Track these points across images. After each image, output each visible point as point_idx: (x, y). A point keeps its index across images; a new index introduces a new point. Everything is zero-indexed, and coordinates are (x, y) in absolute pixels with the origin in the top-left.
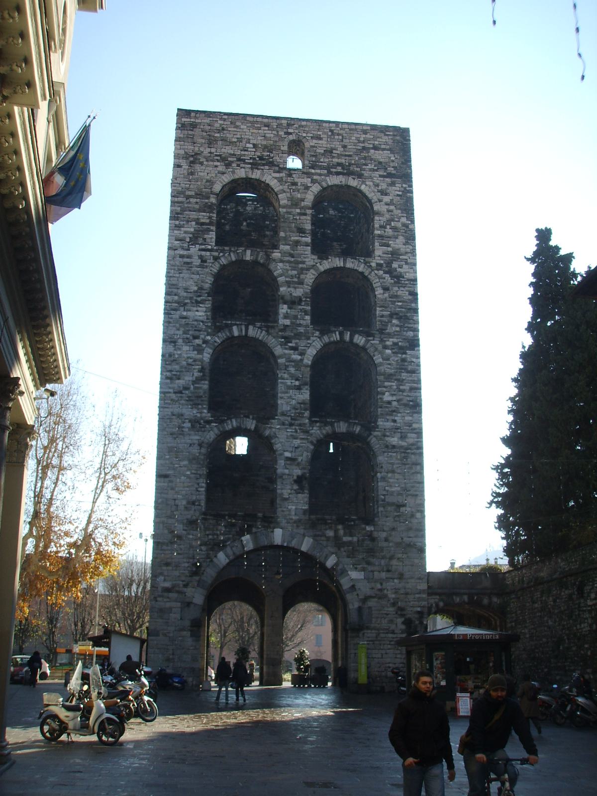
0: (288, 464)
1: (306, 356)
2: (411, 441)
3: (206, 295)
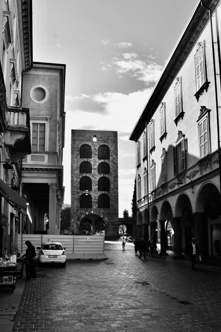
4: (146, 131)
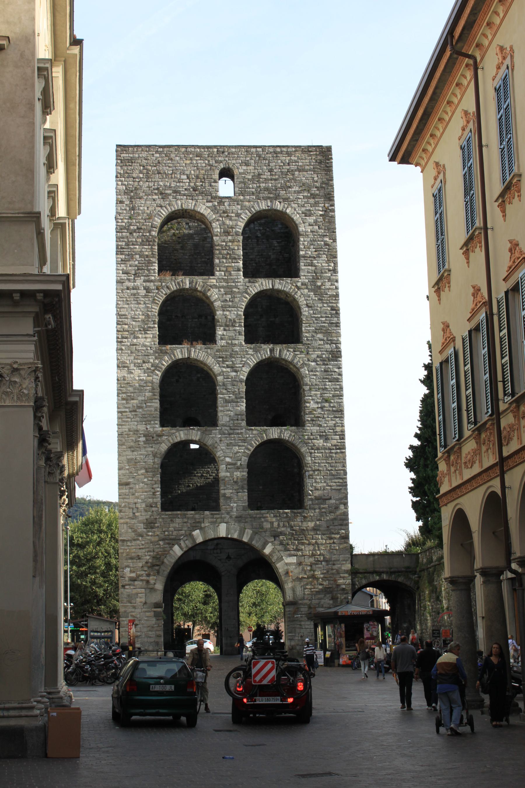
2: (334, 442)
4: (472, 109)
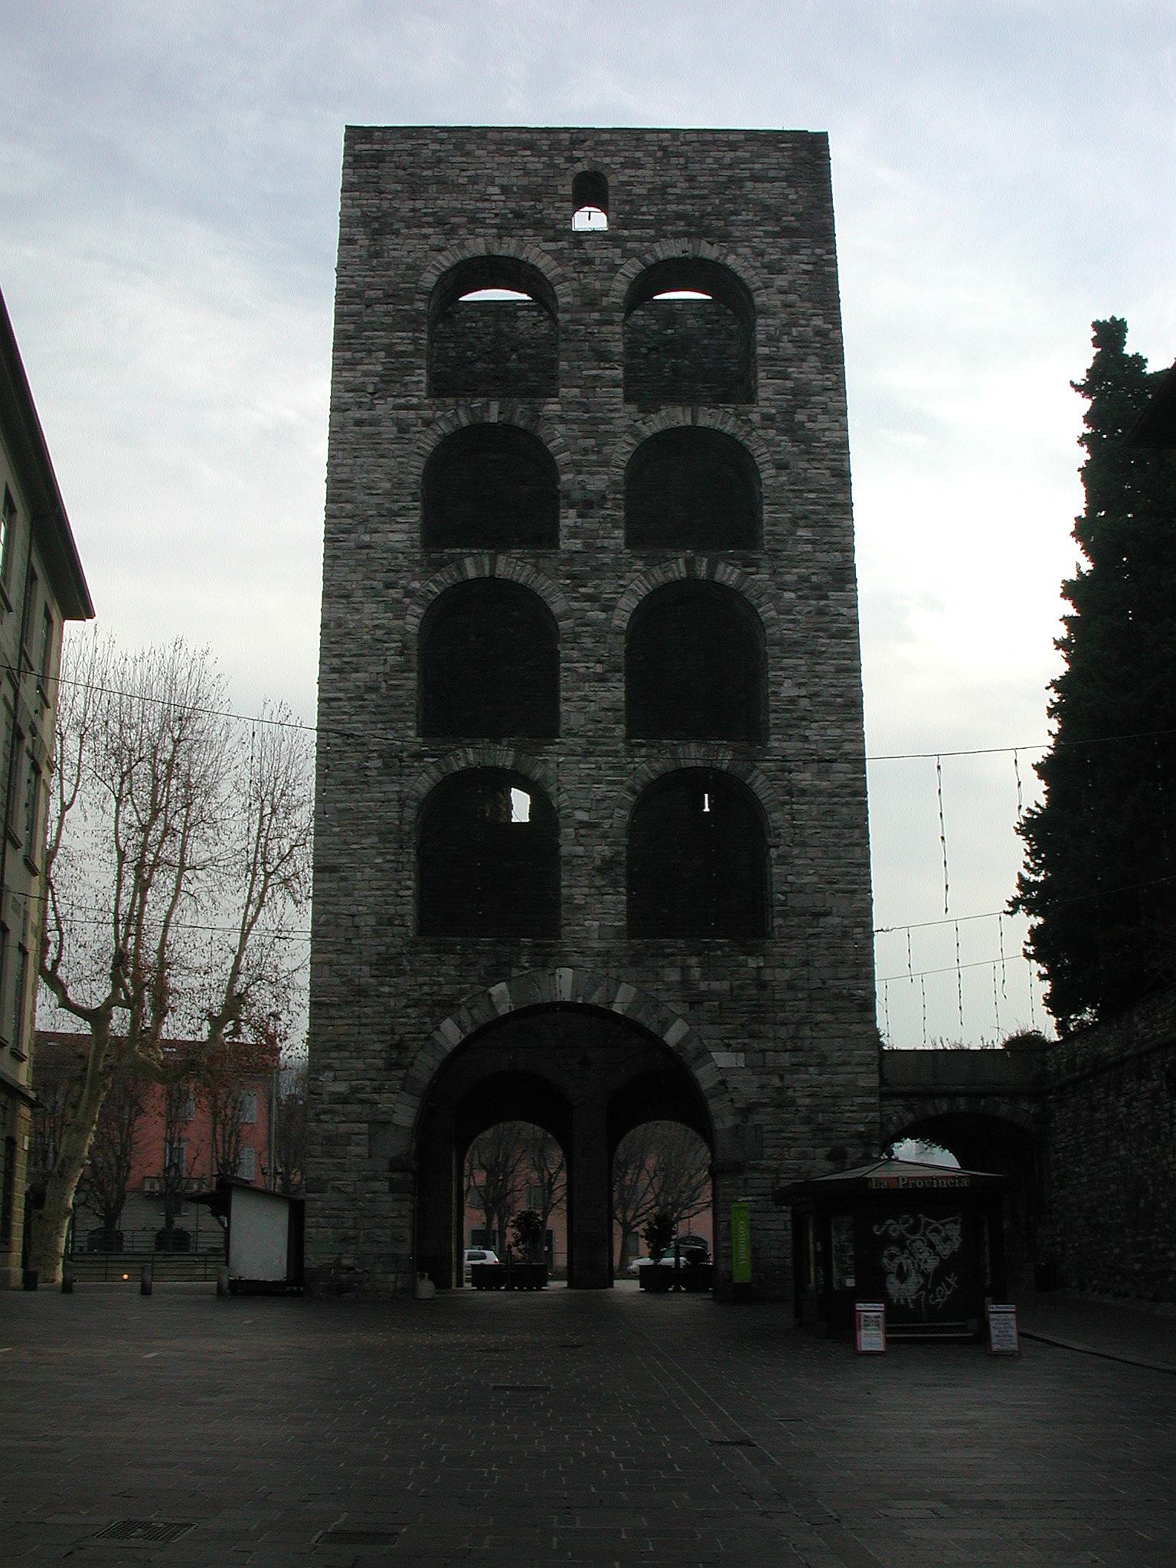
0: (582, 836)
1: (617, 611)
2: (840, 778)
3: (410, 498)
